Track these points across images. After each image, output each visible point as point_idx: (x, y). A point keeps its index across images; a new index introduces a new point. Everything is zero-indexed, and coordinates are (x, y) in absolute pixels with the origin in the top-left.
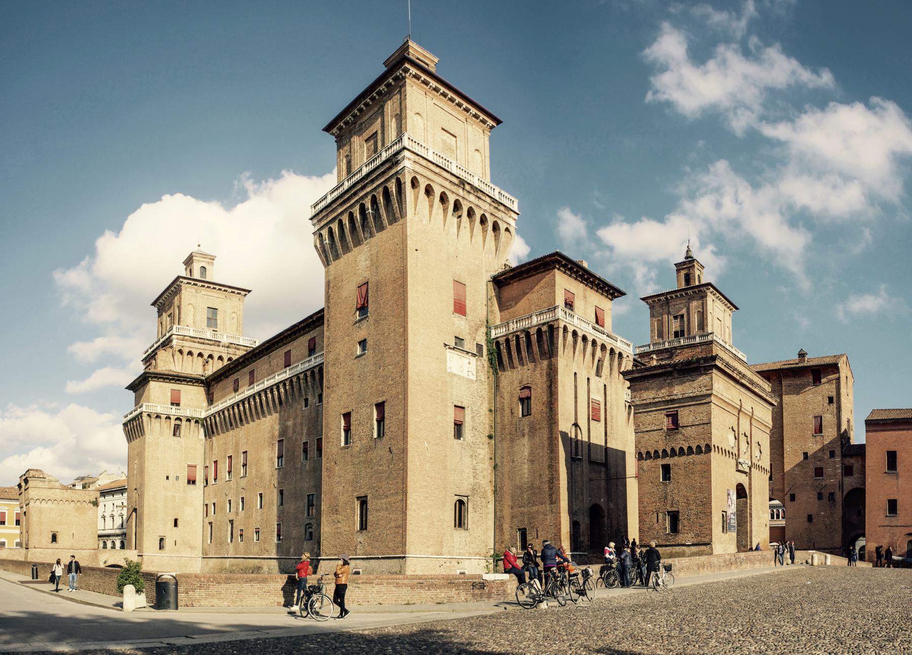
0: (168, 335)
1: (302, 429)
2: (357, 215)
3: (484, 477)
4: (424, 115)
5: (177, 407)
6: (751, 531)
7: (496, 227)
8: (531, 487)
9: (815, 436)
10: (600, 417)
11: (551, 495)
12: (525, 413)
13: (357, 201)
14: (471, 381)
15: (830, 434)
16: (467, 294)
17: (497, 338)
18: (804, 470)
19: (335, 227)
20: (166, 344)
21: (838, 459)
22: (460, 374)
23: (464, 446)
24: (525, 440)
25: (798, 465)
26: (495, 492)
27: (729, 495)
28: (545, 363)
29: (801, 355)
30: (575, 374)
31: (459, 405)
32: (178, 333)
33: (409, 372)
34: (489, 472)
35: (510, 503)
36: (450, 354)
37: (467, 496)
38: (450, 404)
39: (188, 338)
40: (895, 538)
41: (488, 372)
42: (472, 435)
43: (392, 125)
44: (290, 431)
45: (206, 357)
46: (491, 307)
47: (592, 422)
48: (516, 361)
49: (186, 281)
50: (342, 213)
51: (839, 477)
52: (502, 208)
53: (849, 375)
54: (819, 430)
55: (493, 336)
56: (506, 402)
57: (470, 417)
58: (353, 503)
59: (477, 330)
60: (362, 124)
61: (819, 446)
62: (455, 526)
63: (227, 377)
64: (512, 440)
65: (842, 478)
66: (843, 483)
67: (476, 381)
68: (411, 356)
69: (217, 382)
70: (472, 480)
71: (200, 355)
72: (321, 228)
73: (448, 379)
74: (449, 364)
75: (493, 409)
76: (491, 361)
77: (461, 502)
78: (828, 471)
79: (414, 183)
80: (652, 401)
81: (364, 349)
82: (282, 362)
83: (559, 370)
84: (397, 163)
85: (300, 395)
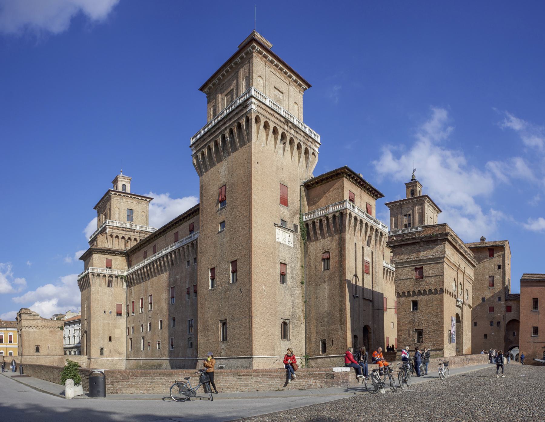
0: (103, 226)
1: (186, 280)
2: (220, 142)
3: (298, 308)
4: (264, 77)
5: (110, 269)
6: (463, 343)
7: (307, 152)
9: (490, 288)
10: (369, 271)
11: (341, 319)
12: (326, 268)
13: (220, 133)
14: (291, 248)
15: (498, 287)
16: (289, 192)
17: (307, 221)
19: (206, 151)
20: (103, 231)
22: (284, 243)
23: (286, 288)
24: (326, 285)
26: (305, 317)
27: (452, 320)
28: (338, 236)
29: (482, 239)
30: (355, 244)
31: (284, 262)
32: (110, 225)
33: (253, 240)
34: (302, 304)
35: (315, 324)
37: (289, 320)
38: (278, 262)
39: (116, 227)
40: (537, 349)
41: (301, 242)
43: (243, 84)
44: (179, 282)
45: (126, 239)
46: (303, 202)
47: (365, 274)
48: (319, 236)
49: (114, 193)
50: (210, 141)
52: (311, 140)
53: (509, 253)
54: (492, 284)
55: (304, 220)
56: (312, 261)
57: (290, 270)
58: (218, 324)
59: (294, 216)
60: (223, 84)
61: (492, 294)
62: (282, 338)
63: (139, 250)
64: (316, 285)
67: (294, 248)
68: (253, 230)
69: (134, 254)
70: (291, 310)
71: (123, 238)
72: (197, 152)
73: (277, 246)
74: (277, 237)
75: (304, 265)
76: (302, 235)
77: (285, 323)
79: (257, 120)
80: (406, 260)
81: (223, 227)
82: (173, 239)
83: (346, 241)
84: (247, 106)
85: (185, 259)
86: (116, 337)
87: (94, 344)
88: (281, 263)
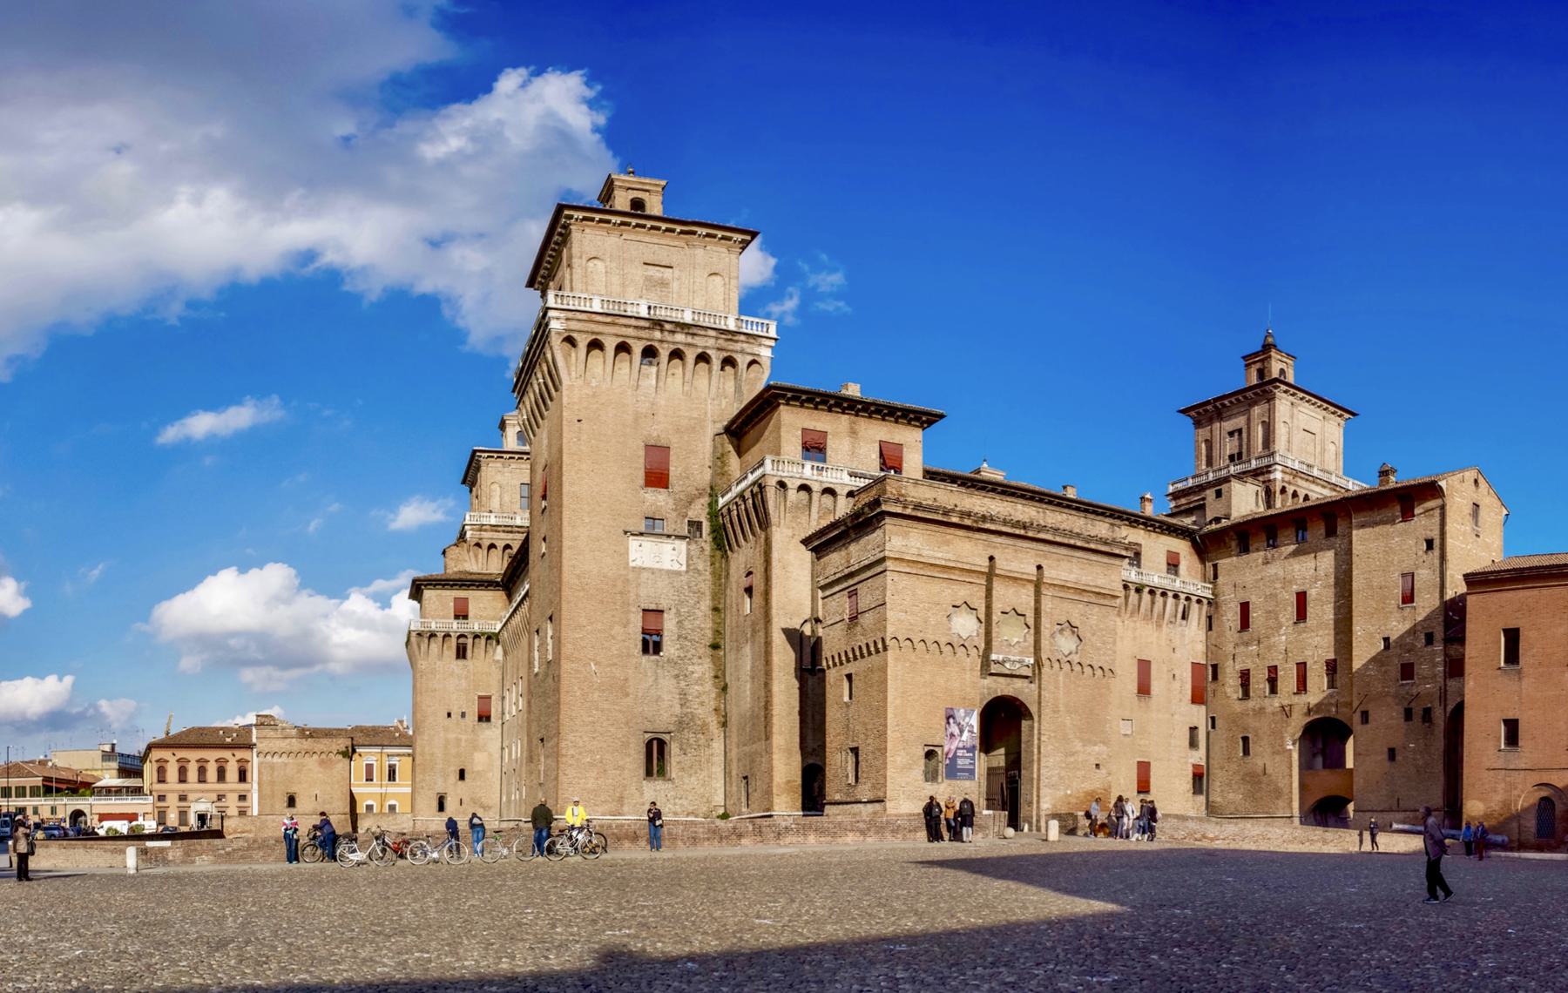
8: (752, 717)
14: (678, 573)
18: (1383, 669)
21: (1439, 647)
22: (657, 566)
23: (660, 664)
25: (1373, 660)
31: (653, 607)
34: (714, 695)
36: (633, 543)
37: (669, 733)
38: (634, 609)
42: (678, 646)
46: (722, 468)
51: (1440, 679)
54: (1408, 598)
57: (674, 622)
59: (690, 503)
61: (1408, 626)
65: (1445, 681)
66: (1446, 691)
67: (687, 572)
70: (677, 710)
73: (631, 576)
74: (631, 557)
78: (1422, 669)
86: (475, 769)
87: (422, 788)
88: (644, 610)
